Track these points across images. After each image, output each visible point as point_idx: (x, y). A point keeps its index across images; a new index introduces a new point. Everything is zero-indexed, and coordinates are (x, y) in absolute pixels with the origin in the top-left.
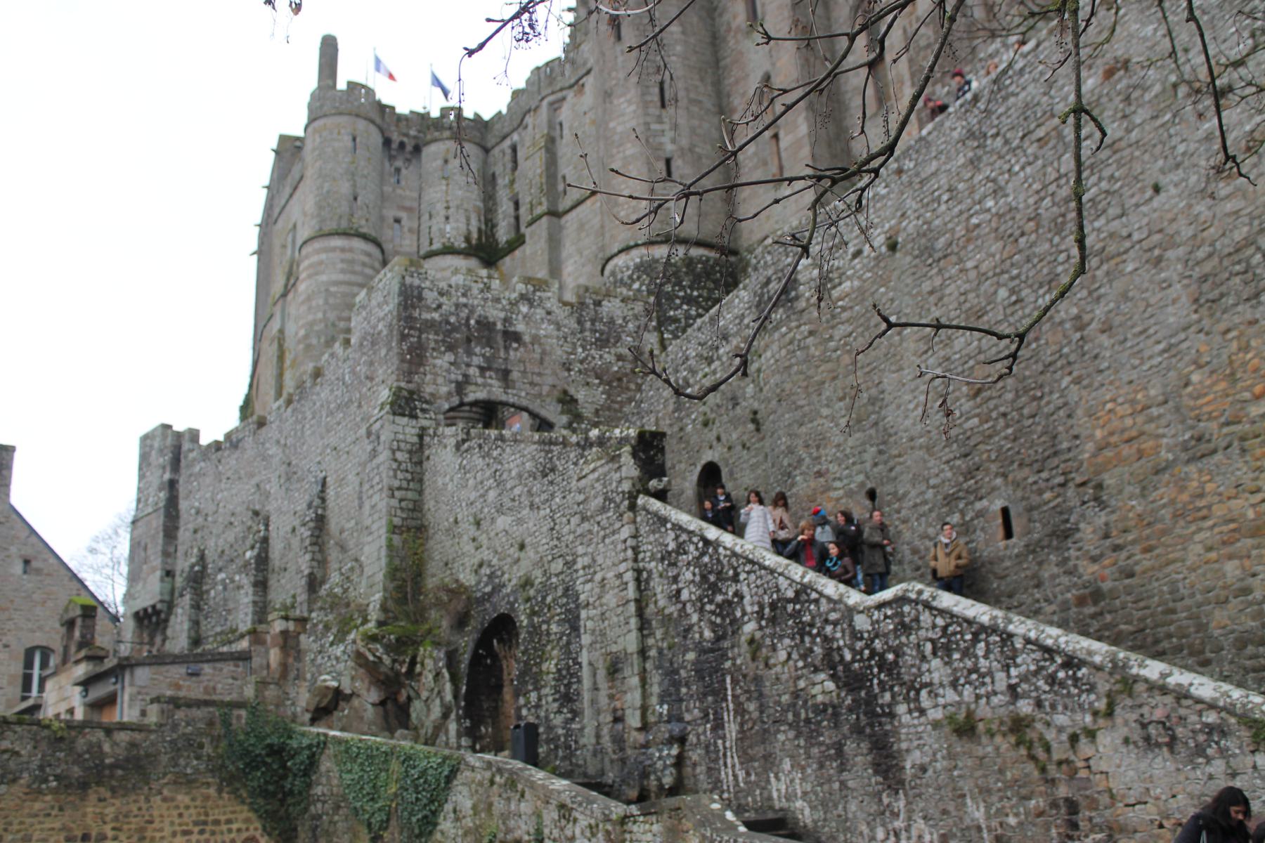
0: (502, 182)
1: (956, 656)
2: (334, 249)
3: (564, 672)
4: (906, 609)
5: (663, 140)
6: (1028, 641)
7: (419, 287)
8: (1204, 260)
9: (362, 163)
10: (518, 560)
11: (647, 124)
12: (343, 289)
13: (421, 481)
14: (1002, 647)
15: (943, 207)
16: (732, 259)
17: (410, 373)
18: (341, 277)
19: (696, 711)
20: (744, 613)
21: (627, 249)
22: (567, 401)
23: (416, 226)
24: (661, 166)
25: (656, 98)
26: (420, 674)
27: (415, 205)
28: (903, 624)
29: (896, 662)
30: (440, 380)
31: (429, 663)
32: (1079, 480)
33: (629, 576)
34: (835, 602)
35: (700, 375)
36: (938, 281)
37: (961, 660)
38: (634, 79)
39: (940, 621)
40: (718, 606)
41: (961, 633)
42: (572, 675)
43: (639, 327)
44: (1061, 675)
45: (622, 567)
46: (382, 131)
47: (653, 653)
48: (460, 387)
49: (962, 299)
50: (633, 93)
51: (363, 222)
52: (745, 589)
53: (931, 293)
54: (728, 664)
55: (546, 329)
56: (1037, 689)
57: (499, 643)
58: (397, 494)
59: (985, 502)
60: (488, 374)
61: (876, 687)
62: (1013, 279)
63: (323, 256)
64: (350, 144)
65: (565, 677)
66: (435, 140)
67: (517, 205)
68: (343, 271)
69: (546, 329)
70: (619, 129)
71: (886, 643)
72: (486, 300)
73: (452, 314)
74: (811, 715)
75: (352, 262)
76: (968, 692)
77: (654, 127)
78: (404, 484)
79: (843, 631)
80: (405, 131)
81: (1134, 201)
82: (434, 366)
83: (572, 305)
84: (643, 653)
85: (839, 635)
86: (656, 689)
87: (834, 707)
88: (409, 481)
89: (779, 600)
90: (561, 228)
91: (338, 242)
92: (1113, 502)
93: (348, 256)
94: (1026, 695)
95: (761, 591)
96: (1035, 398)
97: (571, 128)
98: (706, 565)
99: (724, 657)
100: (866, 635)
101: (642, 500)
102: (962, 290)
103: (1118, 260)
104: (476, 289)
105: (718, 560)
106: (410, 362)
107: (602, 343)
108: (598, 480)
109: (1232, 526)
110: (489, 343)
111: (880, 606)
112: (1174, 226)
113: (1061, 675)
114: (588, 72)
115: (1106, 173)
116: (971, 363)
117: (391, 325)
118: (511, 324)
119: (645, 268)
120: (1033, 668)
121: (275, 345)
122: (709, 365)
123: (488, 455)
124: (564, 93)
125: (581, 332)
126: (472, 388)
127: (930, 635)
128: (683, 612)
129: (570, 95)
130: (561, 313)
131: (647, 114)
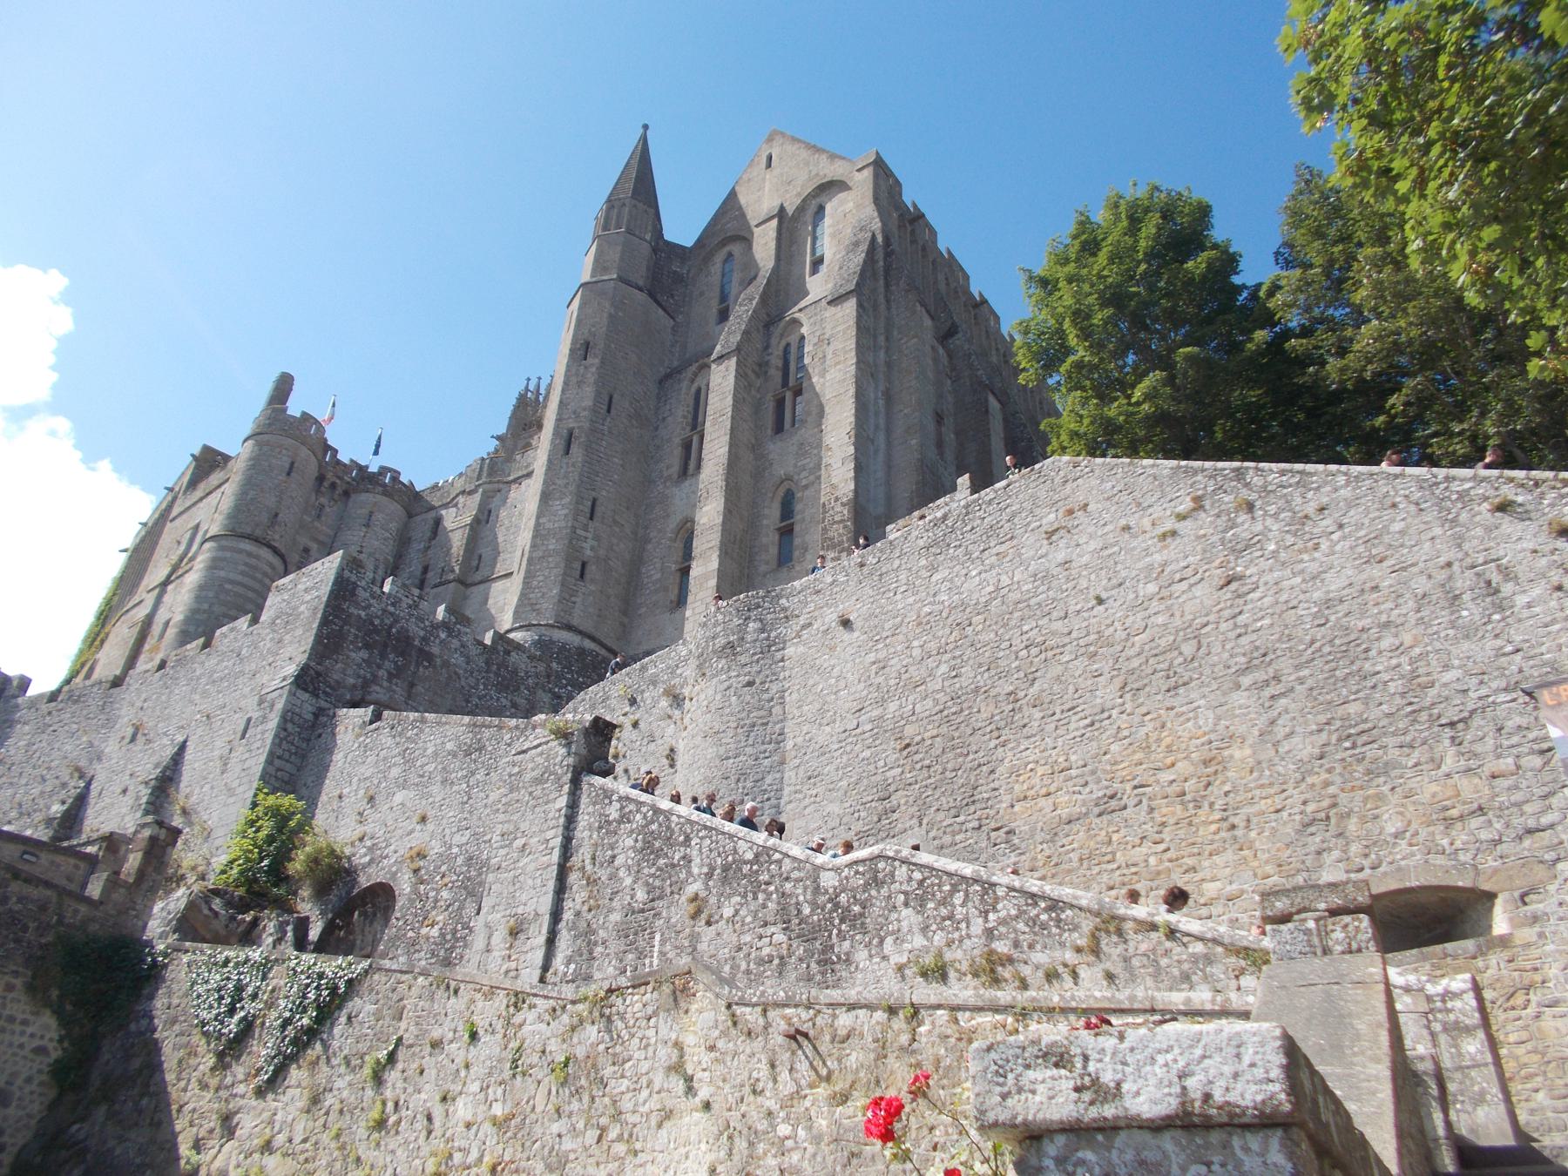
0: (417, 546)
1: (931, 905)
2: (240, 551)
3: (448, 937)
4: (881, 865)
5: (584, 545)
7: (355, 583)
8: (1132, 657)
9: (293, 486)
11: (574, 528)
12: (240, 590)
13: (304, 757)
14: (982, 896)
15: (899, 596)
17: (322, 657)
18: (240, 578)
19: (611, 969)
20: (689, 873)
24: (578, 565)
25: (588, 510)
28: (875, 879)
29: (862, 915)
30: (350, 672)
31: (271, 927)
32: (993, 825)
34: (801, 861)
35: (619, 712)
36: (881, 655)
37: (935, 909)
40: (659, 869)
41: (939, 886)
42: (457, 940)
43: (537, 684)
44: (1044, 917)
45: (550, 834)
46: (320, 466)
49: (904, 670)
51: (277, 537)
52: (695, 853)
54: (659, 923)
55: (457, 659)
56: (1015, 931)
57: (360, 916)
58: (277, 762)
60: (395, 681)
61: (834, 936)
62: (954, 658)
63: (228, 554)
64: (287, 466)
65: (447, 941)
67: (426, 570)
68: (242, 573)
71: (854, 897)
72: (411, 615)
73: (377, 617)
74: (752, 966)
75: (255, 568)
77: (579, 532)
78: (287, 755)
79: (805, 888)
80: (340, 474)
81: (1079, 607)
82: (348, 657)
83: (485, 646)
84: (556, 916)
85: (800, 891)
87: (782, 958)
88: (291, 754)
89: (734, 861)
90: (465, 598)
91: (247, 546)
92: (1023, 845)
93: (253, 561)
95: (715, 854)
96: (961, 755)
100: (831, 891)
102: (904, 663)
103: (1058, 651)
104: (407, 601)
105: (668, 828)
106: (326, 646)
109: (1133, 870)
112: (1111, 629)
113: (1044, 917)
116: (903, 722)
118: (427, 644)
120: (1013, 912)
121: (137, 629)
124: (501, 486)
125: (487, 672)
126: (377, 688)
127: (904, 887)
130: (474, 651)
131: (575, 519)
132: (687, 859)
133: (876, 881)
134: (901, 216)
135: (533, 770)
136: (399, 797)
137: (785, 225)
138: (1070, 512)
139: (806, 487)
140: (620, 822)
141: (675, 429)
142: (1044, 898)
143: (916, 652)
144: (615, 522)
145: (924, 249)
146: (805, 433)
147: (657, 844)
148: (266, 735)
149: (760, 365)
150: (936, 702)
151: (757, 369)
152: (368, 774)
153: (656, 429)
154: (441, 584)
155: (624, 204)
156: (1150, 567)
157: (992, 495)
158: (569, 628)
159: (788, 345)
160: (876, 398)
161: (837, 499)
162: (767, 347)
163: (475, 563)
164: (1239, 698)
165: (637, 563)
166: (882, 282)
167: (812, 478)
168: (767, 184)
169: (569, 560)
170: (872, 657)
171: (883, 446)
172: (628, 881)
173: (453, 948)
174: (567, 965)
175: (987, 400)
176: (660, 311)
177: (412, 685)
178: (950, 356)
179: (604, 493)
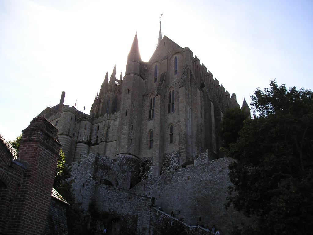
0: (95, 132)
16: (139, 159)
18: (65, 144)
21: (122, 153)
23: (77, 136)
26: (97, 225)
27: (78, 132)
38: (128, 124)
55: (115, 169)
58: (92, 193)
66: (84, 120)
68: (65, 142)
84: (150, 228)
90: (107, 145)
91: (65, 136)
93: (67, 140)
98: (164, 218)
107: (123, 173)
108: (144, 202)
111: (194, 228)
117: (93, 163)
119: (125, 158)
129: (113, 120)
130: (118, 166)
132: (170, 223)
139: (175, 126)
140: (159, 215)
146: (175, 114)
147: (165, 220)
148: (89, 188)
151: (164, 97)
152: (110, 197)
154: (102, 142)
157: (212, 162)
158: (130, 154)
159: (170, 92)
162: (166, 92)
165: (140, 139)
166: (190, 82)
169: (129, 139)
170: (193, 186)
175: (210, 103)
177: (109, 175)
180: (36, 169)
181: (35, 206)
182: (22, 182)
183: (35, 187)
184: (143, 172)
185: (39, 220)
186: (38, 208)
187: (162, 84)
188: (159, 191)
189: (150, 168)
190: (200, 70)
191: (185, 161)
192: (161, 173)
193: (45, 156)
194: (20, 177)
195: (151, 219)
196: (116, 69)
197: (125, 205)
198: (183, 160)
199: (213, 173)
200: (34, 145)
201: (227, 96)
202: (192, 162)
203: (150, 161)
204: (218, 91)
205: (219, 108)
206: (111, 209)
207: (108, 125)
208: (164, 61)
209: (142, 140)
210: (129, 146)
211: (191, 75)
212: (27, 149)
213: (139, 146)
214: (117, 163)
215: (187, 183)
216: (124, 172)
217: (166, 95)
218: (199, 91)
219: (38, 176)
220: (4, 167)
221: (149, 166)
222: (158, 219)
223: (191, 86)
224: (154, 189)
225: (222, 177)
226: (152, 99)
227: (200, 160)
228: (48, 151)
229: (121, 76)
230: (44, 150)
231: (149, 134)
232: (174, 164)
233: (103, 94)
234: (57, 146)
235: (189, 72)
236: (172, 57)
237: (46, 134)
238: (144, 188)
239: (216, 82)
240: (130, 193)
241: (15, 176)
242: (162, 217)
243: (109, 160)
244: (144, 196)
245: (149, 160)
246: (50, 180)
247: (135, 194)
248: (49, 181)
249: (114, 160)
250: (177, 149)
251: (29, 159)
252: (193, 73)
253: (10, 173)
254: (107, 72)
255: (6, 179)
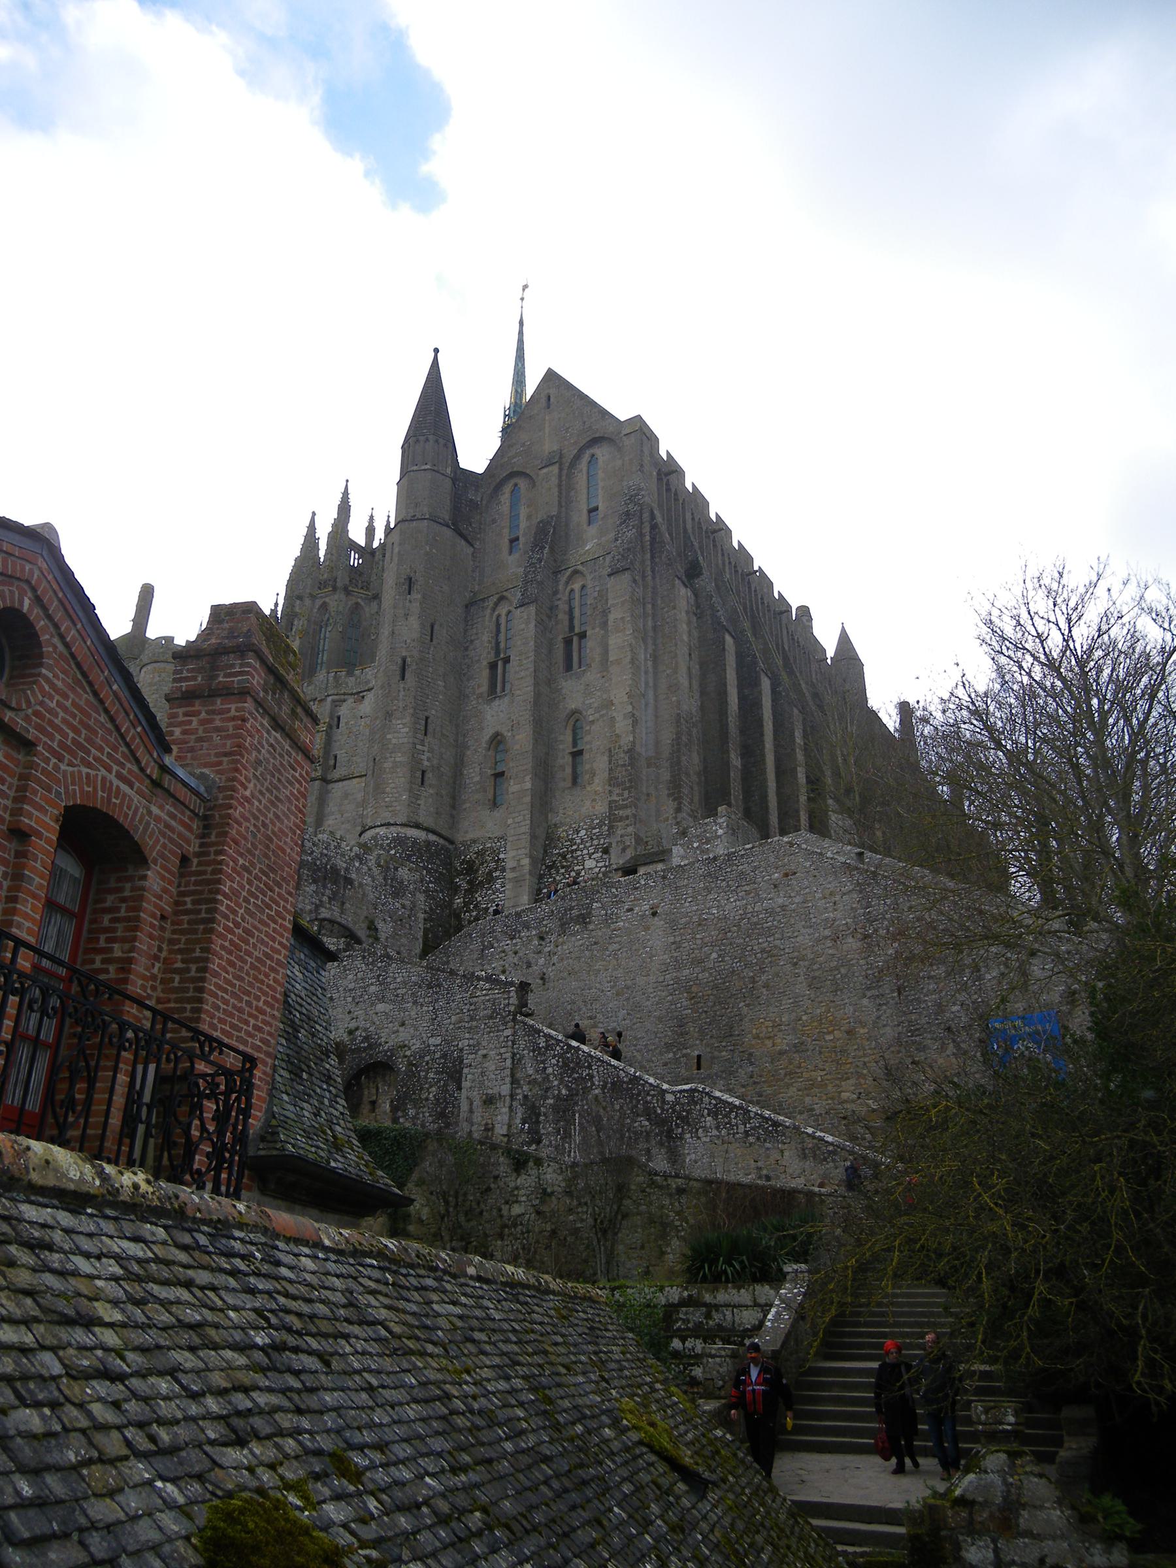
6: (757, 1114)
10: (398, 1031)
11: (414, 744)
16: (451, 847)
20: (593, 1084)
21: (389, 824)
22: (372, 927)
24: (419, 774)
29: (687, 1116)
33: (509, 1055)
36: (678, 939)
38: (411, 711)
39: (714, 1102)
45: (503, 1050)
47: (520, 1097)
48: (317, 907)
50: (407, 720)
53: (673, 943)
55: (367, 880)
59: (689, 1051)
69: (367, 880)
70: (394, 741)
76: (724, 1132)
77: (419, 747)
84: (512, 1096)
86: (519, 1115)
90: (328, 792)
94: (752, 1135)
97: (347, 723)
99: (576, 1104)
101: (519, 1017)
107: (396, 894)
110: (335, 883)
111: (681, 1091)
114: (369, 690)
115: (778, 918)
119: (399, 841)
122: (512, 939)
123: (372, 963)
126: (323, 910)
128: (546, 1078)
129: (351, 700)
132: (592, 1077)
133: (696, 1103)
134: (659, 474)
135: (485, 1009)
136: (381, 1007)
137: (565, 472)
138: (786, 875)
139: (592, 722)
141: (483, 651)
142: (770, 1119)
143: (699, 942)
144: (443, 735)
145: (676, 494)
146: (592, 676)
149: (551, 609)
150: (711, 974)
152: (351, 986)
153: (466, 649)
155: (427, 440)
156: (827, 919)
158: (417, 826)
159: (572, 590)
160: (646, 659)
161: (620, 747)
162: (556, 593)
163: (332, 762)
164: (865, 1001)
166: (648, 556)
167: (597, 715)
168: (547, 425)
170: (671, 939)
171: (652, 701)
172: (556, 1083)
173: (446, 1107)
174: (523, 1124)
176: (463, 542)
177: (343, 903)
178: (696, 595)
179: (433, 712)
180: (247, 800)
181: (247, 942)
182: (197, 849)
183: (244, 867)
184: (471, 891)
185: (258, 999)
186: (256, 953)
187: (540, 560)
188: (542, 961)
189: (497, 878)
190: (683, 508)
191: (629, 853)
192: (538, 897)
193: (269, 752)
194: (190, 829)
195: (517, 1061)
196: (352, 502)
197: (413, 1013)
198: (624, 850)
199: (748, 893)
200: (233, 707)
201: (781, 613)
202: (661, 855)
203: (495, 852)
204: (750, 591)
205: (754, 656)
206: (357, 1029)
207: (331, 718)
208: (545, 470)
209: (462, 774)
210: (414, 797)
211: (654, 527)
212: (202, 722)
213: (454, 798)
214: (372, 859)
215: (647, 928)
216: (398, 891)
217: (557, 603)
218: (683, 591)
219: (252, 828)
220: (137, 784)
221: (490, 873)
222: (543, 1062)
223: (653, 571)
224: (521, 954)
225: (783, 907)
226: (499, 616)
227: (695, 845)
228: (278, 735)
229: (370, 531)
230: (268, 732)
231: (491, 753)
232: (589, 864)
233: (300, 598)
234: (305, 719)
235: (646, 515)
236: (577, 457)
237: (271, 670)
238: (483, 950)
239: (744, 556)
240: (431, 968)
241: (173, 823)
242: (561, 1056)
243: (343, 844)
244: (488, 979)
245: (491, 847)
246: (288, 851)
247: (452, 973)
248: (284, 851)
249: (360, 845)
250: (601, 808)
251: (220, 763)
252: (659, 519)
253: (155, 810)
254: (314, 514)
255: (145, 829)
